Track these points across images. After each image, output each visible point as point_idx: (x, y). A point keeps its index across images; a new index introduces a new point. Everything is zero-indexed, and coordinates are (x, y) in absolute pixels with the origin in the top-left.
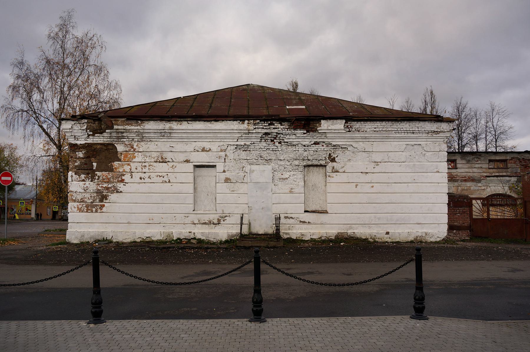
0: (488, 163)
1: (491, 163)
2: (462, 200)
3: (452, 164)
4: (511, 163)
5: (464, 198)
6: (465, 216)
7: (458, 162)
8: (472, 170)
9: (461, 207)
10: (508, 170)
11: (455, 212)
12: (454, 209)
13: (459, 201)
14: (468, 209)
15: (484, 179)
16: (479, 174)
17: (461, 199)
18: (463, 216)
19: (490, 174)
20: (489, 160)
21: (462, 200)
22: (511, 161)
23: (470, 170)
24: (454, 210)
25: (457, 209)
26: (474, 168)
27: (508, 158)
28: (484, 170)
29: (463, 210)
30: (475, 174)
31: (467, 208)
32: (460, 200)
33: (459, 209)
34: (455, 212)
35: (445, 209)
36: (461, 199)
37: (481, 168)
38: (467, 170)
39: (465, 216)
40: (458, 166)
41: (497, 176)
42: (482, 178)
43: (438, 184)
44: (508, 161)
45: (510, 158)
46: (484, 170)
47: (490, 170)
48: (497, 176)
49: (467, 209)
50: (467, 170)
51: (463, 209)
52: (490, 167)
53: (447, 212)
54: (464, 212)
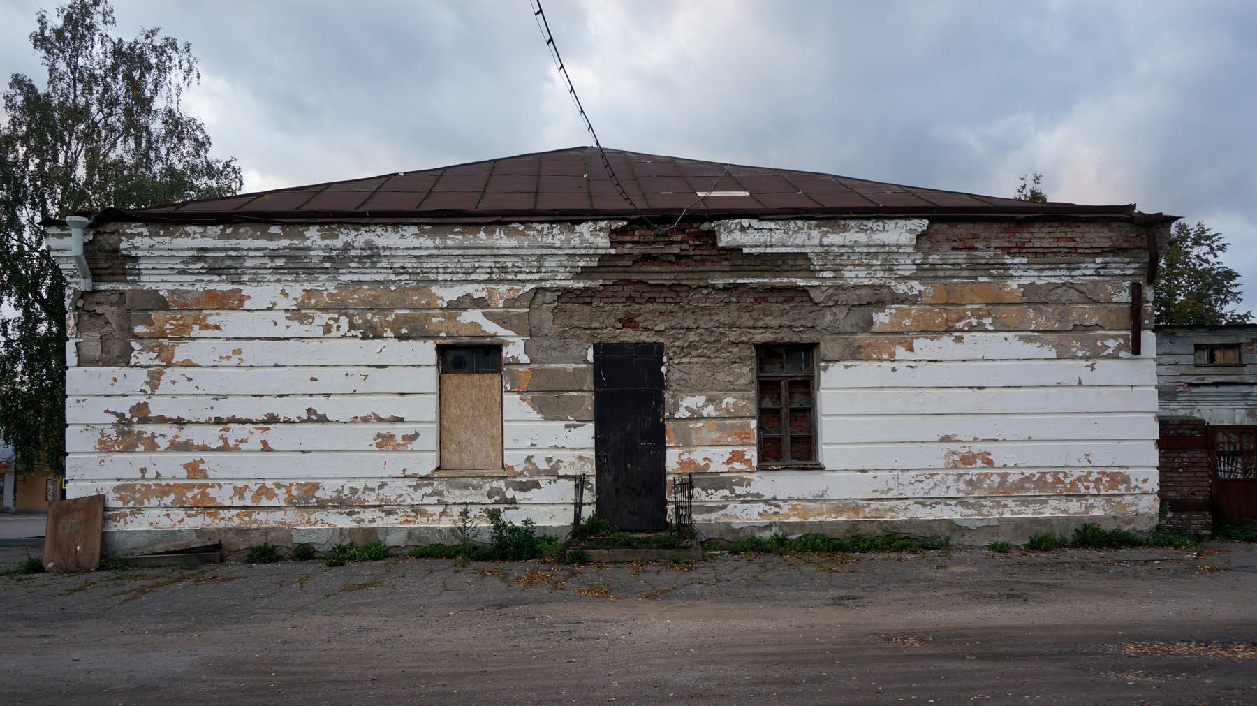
1: (1200, 352)
2: (1186, 431)
5: (1192, 426)
6: (1197, 474)
9: (1185, 450)
10: (1244, 368)
11: (1168, 464)
12: (1166, 455)
13: (1180, 434)
14: (1204, 455)
15: (1184, 392)
16: (1172, 379)
17: (1184, 430)
18: (1193, 474)
19: (1197, 379)
21: (1186, 431)
24: (1168, 457)
25: (1176, 455)
27: (1243, 340)
28: (1184, 370)
29: (1190, 458)
31: (1201, 452)
32: (1181, 431)
33: (1179, 457)
34: (1168, 464)
35: (1153, 456)
36: (1184, 430)
37: (1176, 364)
39: (1197, 474)
41: (1217, 384)
42: (1181, 389)
43: (1130, 389)
44: (1243, 347)
45: (1249, 341)
46: (1184, 370)
48: (1217, 384)
49: (1200, 455)
51: (1191, 455)
53: (1157, 463)
54: (1195, 463)
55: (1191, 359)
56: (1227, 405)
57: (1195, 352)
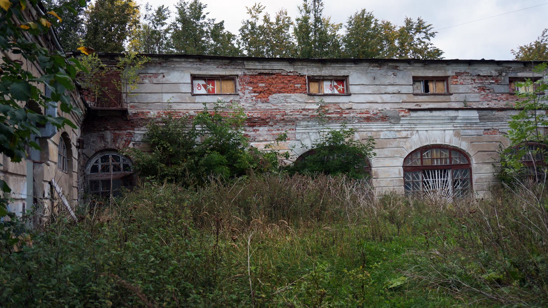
0: (412, 83)
1: (417, 84)
3: (341, 87)
4: (456, 84)
7: (351, 80)
8: (381, 98)
10: (451, 97)
15: (406, 116)
16: (396, 106)
20: (413, 77)
22: (455, 80)
23: (377, 98)
26: (385, 93)
28: (405, 97)
30: (388, 107)
37: (399, 93)
38: (371, 98)
40: (352, 89)
41: (431, 110)
42: (402, 113)
44: (450, 79)
45: (454, 74)
46: (405, 97)
47: (416, 98)
48: (431, 110)
50: (371, 98)
52: (417, 92)
55: (410, 89)
56: (439, 127)
57: (414, 84)
